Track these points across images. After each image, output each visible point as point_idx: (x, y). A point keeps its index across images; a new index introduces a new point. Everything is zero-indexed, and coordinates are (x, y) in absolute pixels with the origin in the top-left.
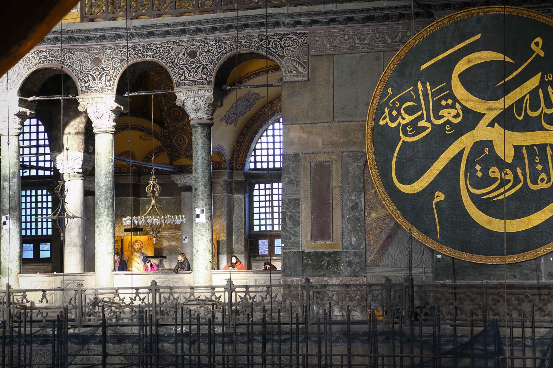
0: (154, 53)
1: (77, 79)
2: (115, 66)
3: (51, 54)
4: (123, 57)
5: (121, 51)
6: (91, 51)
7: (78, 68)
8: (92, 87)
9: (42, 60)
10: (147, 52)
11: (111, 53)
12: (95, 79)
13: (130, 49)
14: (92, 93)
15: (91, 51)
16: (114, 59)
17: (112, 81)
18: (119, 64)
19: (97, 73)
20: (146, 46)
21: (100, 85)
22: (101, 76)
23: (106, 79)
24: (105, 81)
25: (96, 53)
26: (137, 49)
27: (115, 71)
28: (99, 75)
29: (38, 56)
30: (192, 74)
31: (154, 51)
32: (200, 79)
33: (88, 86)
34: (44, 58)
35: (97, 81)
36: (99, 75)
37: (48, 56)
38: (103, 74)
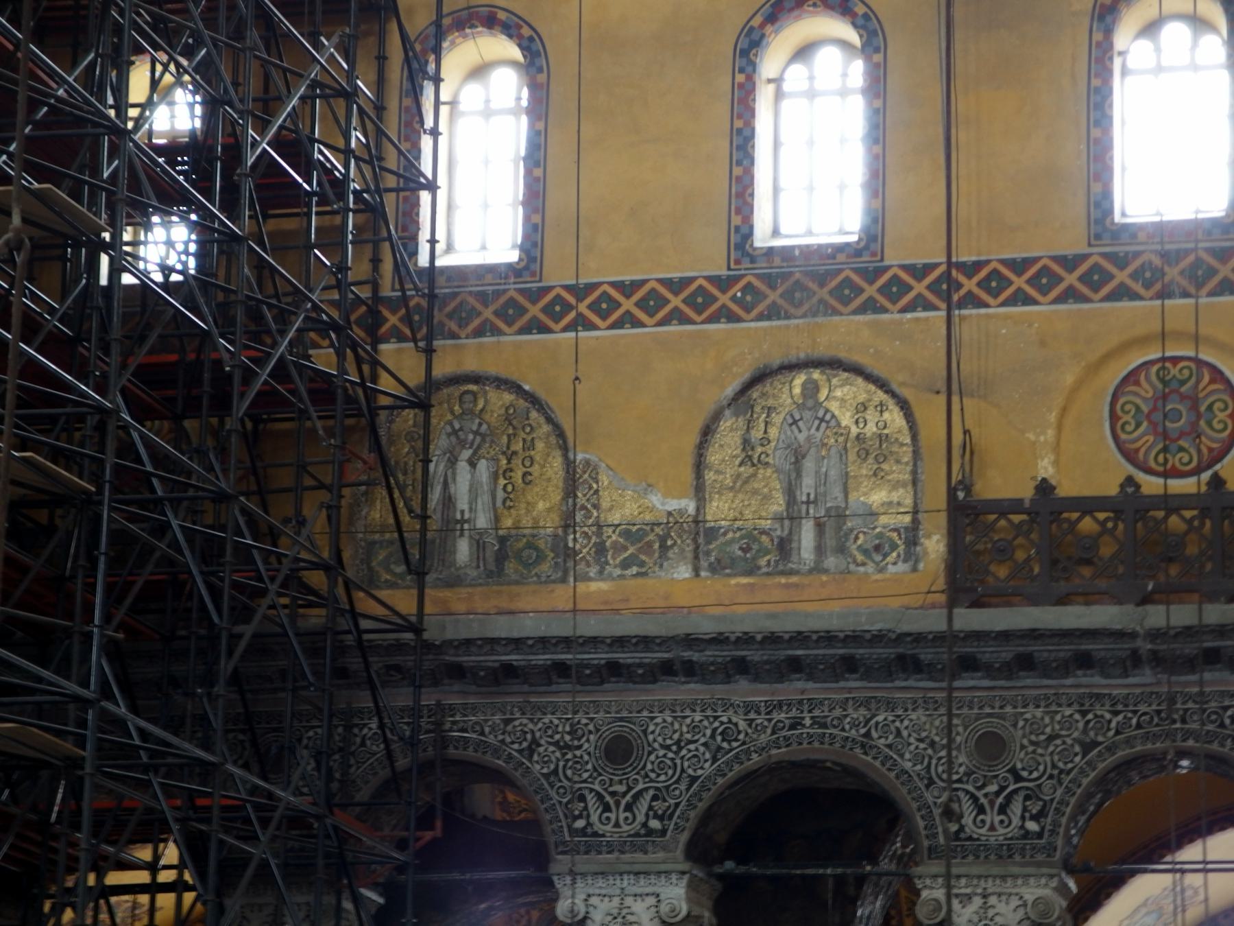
0: (1210, 727)
1: (915, 805)
2: (1061, 765)
3: (816, 713)
4: (1092, 734)
5: (1084, 713)
6: (971, 708)
7: (919, 767)
8: (970, 838)
9: (784, 733)
10: (1184, 721)
11: (1047, 720)
12: (981, 810)
13: (1120, 707)
14: (971, 858)
15: (971, 708)
16: (1058, 742)
17: (1049, 820)
18: (1077, 759)
19: (993, 788)
20: (1180, 700)
21: (1001, 831)
22: (1009, 799)
23: (1025, 809)
24: (1023, 818)
25: (989, 715)
26: (1147, 710)
27: (1060, 783)
28: (998, 794)
29: (770, 720)
30: (613, 816)
31: (1214, 717)
32: (637, 835)
33: (957, 832)
34: (793, 727)
35: (992, 817)
36: (998, 794)
37: (808, 722)
38: (1015, 791)
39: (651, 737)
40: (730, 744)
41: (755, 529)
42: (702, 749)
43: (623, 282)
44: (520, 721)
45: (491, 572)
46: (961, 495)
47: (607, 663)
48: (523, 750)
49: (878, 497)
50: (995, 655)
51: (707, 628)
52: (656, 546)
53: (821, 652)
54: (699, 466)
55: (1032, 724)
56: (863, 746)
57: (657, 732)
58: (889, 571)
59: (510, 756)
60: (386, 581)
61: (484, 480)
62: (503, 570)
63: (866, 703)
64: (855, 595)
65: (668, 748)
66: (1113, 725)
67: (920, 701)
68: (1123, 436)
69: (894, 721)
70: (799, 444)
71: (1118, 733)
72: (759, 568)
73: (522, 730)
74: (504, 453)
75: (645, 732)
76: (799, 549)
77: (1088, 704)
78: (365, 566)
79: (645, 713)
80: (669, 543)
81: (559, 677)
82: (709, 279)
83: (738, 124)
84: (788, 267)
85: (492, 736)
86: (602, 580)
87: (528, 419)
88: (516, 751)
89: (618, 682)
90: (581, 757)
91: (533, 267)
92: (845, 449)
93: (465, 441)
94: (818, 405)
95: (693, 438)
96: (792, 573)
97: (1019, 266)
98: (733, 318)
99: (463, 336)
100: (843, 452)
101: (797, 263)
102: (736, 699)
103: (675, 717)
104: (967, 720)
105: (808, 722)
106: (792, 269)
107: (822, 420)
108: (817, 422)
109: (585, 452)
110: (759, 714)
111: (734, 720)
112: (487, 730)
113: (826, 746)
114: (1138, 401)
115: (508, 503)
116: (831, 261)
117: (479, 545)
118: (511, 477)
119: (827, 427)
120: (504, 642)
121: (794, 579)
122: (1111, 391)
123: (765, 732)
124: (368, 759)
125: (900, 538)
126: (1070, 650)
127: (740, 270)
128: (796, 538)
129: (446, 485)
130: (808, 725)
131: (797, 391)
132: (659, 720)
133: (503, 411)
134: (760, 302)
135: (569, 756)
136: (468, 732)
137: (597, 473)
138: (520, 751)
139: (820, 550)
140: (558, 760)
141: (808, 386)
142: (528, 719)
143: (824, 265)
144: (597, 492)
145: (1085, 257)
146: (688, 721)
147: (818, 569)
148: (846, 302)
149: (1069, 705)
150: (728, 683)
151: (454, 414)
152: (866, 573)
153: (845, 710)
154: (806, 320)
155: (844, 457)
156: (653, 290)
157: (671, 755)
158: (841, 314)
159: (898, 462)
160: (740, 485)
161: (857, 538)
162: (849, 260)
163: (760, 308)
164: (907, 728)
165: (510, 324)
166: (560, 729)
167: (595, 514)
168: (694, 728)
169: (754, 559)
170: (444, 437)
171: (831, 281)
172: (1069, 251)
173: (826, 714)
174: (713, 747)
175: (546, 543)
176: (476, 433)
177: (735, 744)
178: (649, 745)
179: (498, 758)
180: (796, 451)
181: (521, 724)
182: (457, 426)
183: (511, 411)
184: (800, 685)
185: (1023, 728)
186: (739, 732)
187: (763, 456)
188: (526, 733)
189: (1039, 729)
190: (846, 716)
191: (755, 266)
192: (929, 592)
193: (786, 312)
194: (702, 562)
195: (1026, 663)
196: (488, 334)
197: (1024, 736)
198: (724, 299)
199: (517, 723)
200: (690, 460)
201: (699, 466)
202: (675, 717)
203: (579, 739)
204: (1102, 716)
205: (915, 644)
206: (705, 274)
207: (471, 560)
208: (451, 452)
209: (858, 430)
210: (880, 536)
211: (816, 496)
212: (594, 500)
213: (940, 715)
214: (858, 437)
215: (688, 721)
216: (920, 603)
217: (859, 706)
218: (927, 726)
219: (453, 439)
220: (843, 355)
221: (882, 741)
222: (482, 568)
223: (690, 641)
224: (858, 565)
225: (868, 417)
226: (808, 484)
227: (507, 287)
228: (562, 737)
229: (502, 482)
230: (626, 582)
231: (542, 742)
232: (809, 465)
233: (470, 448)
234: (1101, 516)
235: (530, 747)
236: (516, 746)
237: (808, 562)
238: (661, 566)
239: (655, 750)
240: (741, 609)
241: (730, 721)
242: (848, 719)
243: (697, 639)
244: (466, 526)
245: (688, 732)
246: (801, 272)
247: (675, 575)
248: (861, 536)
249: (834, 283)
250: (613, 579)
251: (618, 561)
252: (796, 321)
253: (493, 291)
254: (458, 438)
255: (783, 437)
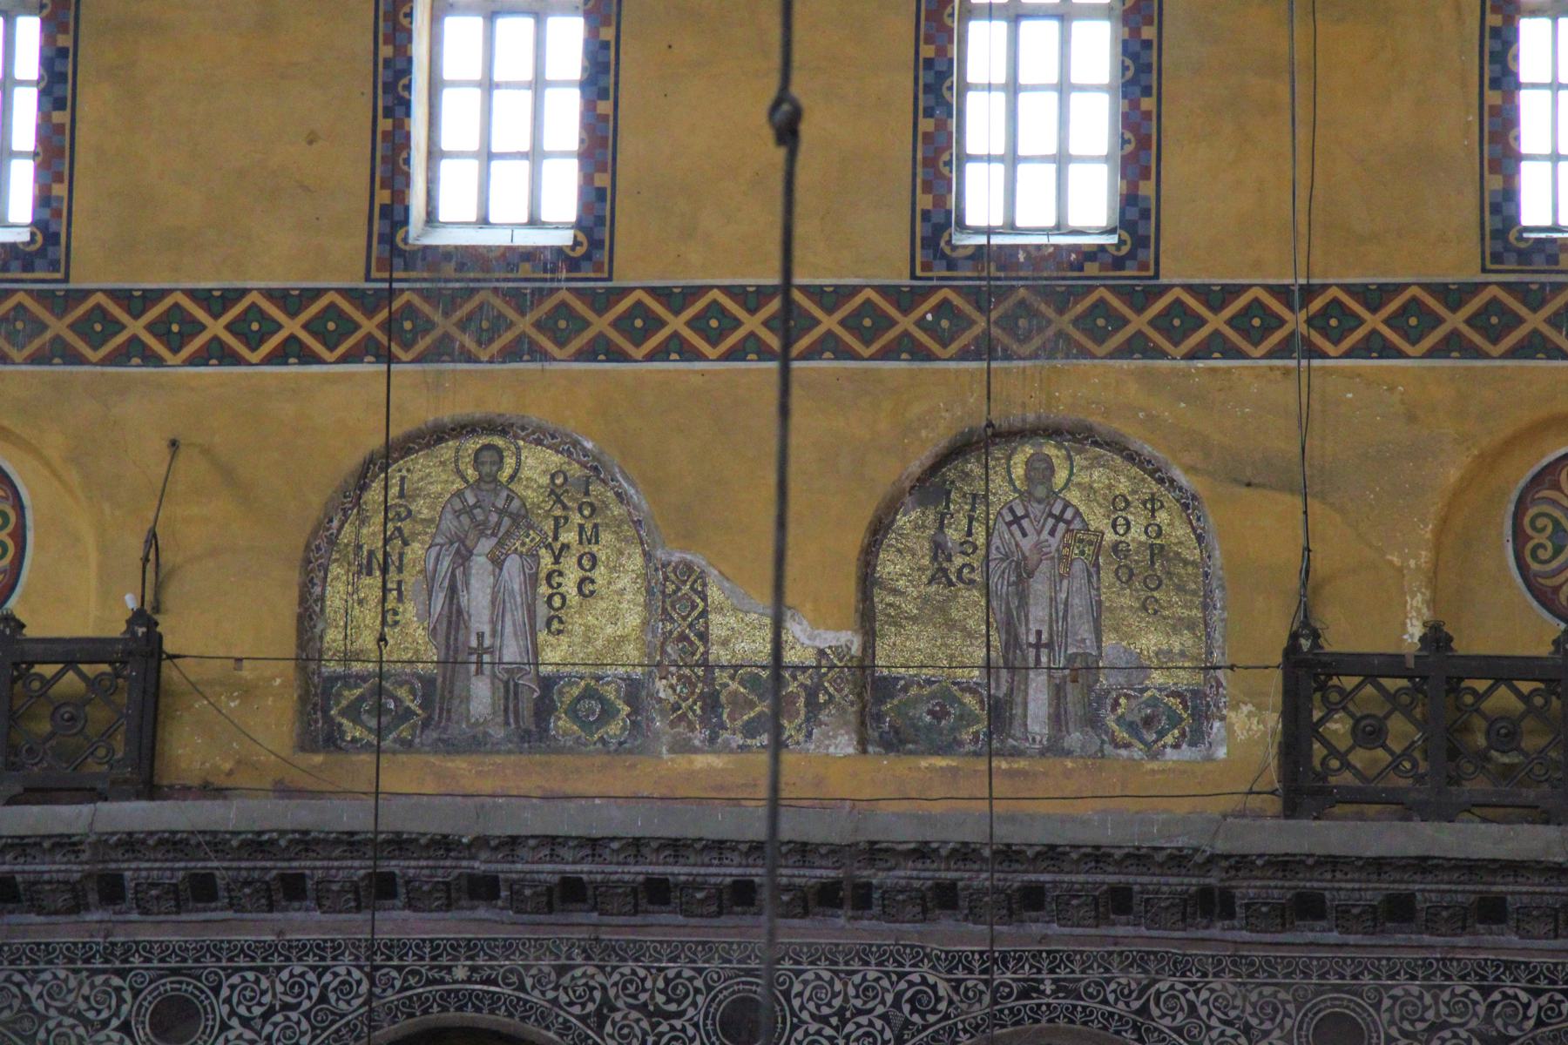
3: (1062, 973)
4: (1499, 1023)
5: (1485, 992)
6: (1307, 975)
9: (1010, 1003)
11: (1428, 999)
13: (1543, 984)
25: (1336, 988)
34: (1024, 994)
37: (1048, 987)
39: (796, 1003)
40: (924, 1018)
41: (954, 683)
42: (879, 1024)
43: (744, 287)
44: (583, 970)
45: (528, 732)
46: (1305, 644)
47: (735, 882)
48: (588, 1015)
49: (1150, 641)
50: (1357, 895)
51: (906, 834)
52: (801, 702)
53: (1081, 878)
54: (867, 581)
55: (1403, 1005)
56: (1136, 1028)
57: (807, 994)
58: (1167, 757)
59: (567, 1026)
60: (354, 740)
61: (516, 587)
62: (547, 730)
63: (1141, 961)
64: (1118, 792)
65: (825, 1020)
66: (1533, 1011)
67: (1226, 962)
68: (1535, 566)
69: (1184, 992)
70: (1023, 554)
71: (1540, 1023)
72: (961, 744)
73: (586, 984)
74: (549, 547)
75: (787, 994)
76: (1025, 716)
77: (1491, 977)
78: (319, 714)
79: (787, 964)
80: (822, 698)
81: (651, 902)
82: (882, 290)
83: (928, 51)
84: (1006, 279)
85: (536, 993)
86: (714, 752)
87: (587, 493)
88: (577, 1017)
89: (744, 913)
90: (684, 1030)
91: (1141, 254)
92: (1097, 565)
93: (485, 522)
94: (1053, 495)
95: (855, 539)
96: (1016, 753)
97: (1374, 296)
98: (920, 353)
99: (486, 359)
100: (1093, 570)
101: (1022, 274)
102: (933, 947)
103: (836, 973)
104: (1301, 993)
105: (1048, 987)
106: (1014, 283)
107: (1059, 519)
108: (1051, 521)
109: (684, 550)
110: (971, 972)
111: (931, 979)
112: (529, 982)
113: (1078, 1026)
114: (1558, 514)
115: (555, 625)
116: (1076, 274)
117: (509, 691)
118: (560, 585)
119: (1068, 531)
120: (532, 842)
121: (1021, 764)
122: (1514, 495)
123: (980, 1001)
124: (333, 1022)
125: (1185, 708)
126: (1474, 892)
127: (930, 279)
128: (1019, 699)
129: (453, 590)
130: (1048, 992)
131: (1019, 471)
132: (810, 976)
133: (545, 480)
134: (964, 330)
135: (664, 1027)
136: (498, 985)
137: (704, 585)
138: (583, 1019)
139: (1057, 719)
140: (645, 1033)
141: (1037, 465)
142: (597, 966)
143: (1064, 278)
144: (704, 614)
145: (1478, 287)
146: (857, 979)
147: (1054, 749)
148: (1100, 337)
149: (1463, 978)
150: (924, 920)
151: (467, 481)
152: (1131, 759)
153: (1107, 970)
154: (1038, 362)
155: (1094, 579)
156: (1414, 299)
157: (828, 1031)
158: (1094, 357)
159: (1180, 589)
160: (938, 613)
161: (1116, 704)
162: (1103, 274)
163: (965, 339)
164: (1205, 1002)
165: (561, 344)
166: (648, 984)
167: (702, 649)
168: (865, 990)
169: (953, 729)
170: (449, 516)
171: (1076, 303)
172: (1453, 278)
173: (1078, 976)
174: (898, 1022)
175: (618, 691)
176: (502, 512)
177: (931, 1018)
178: (793, 1014)
179: (547, 1028)
180: (1018, 564)
181: (584, 974)
182: (471, 500)
183: (559, 481)
184: (1036, 929)
185: (1390, 1009)
186: (939, 999)
187: (965, 571)
188: (592, 989)
189: (1415, 1012)
190: (1108, 981)
191: (954, 274)
192: (1251, 792)
193: (1005, 350)
194: (870, 731)
195: (1400, 910)
196: (674, 356)
197: (1392, 1022)
198: (906, 323)
199: (578, 973)
200: (852, 569)
201: (867, 581)
202: (836, 973)
203: (679, 1003)
204: (1516, 997)
205: (1233, 873)
206: (876, 282)
207: (494, 713)
208: (463, 542)
209: (1117, 537)
210: (1154, 702)
211: (1051, 635)
212: (700, 626)
213: (1259, 985)
214: (1115, 547)
215: (857, 979)
216: (1240, 806)
217: (1131, 965)
218: (1238, 1002)
219: (465, 519)
220: (1095, 420)
221: (1167, 1021)
222: (513, 726)
223: (874, 853)
224: (1117, 746)
225: (1130, 517)
226: (1038, 617)
227: (555, 285)
228: (652, 997)
229: (544, 589)
230: (751, 757)
231: (620, 1004)
232: (1039, 586)
233: (494, 535)
234: (1525, 687)
235: (599, 1010)
236: (577, 1010)
237: (1038, 738)
238: (809, 735)
239: (802, 1022)
240: (938, 808)
241: (924, 981)
242: (1113, 986)
243: (886, 850)
244: (486, 658)
245: (857, 996)
246: (1026, 287)
247: (832, 750)
248: (1122, 701)
249: (1080, 308)
250: (731, 751)
251: (739, 723)
252: (1021, 364)
253: (533, 291)
254: (473, 518)
255: (996, 541)
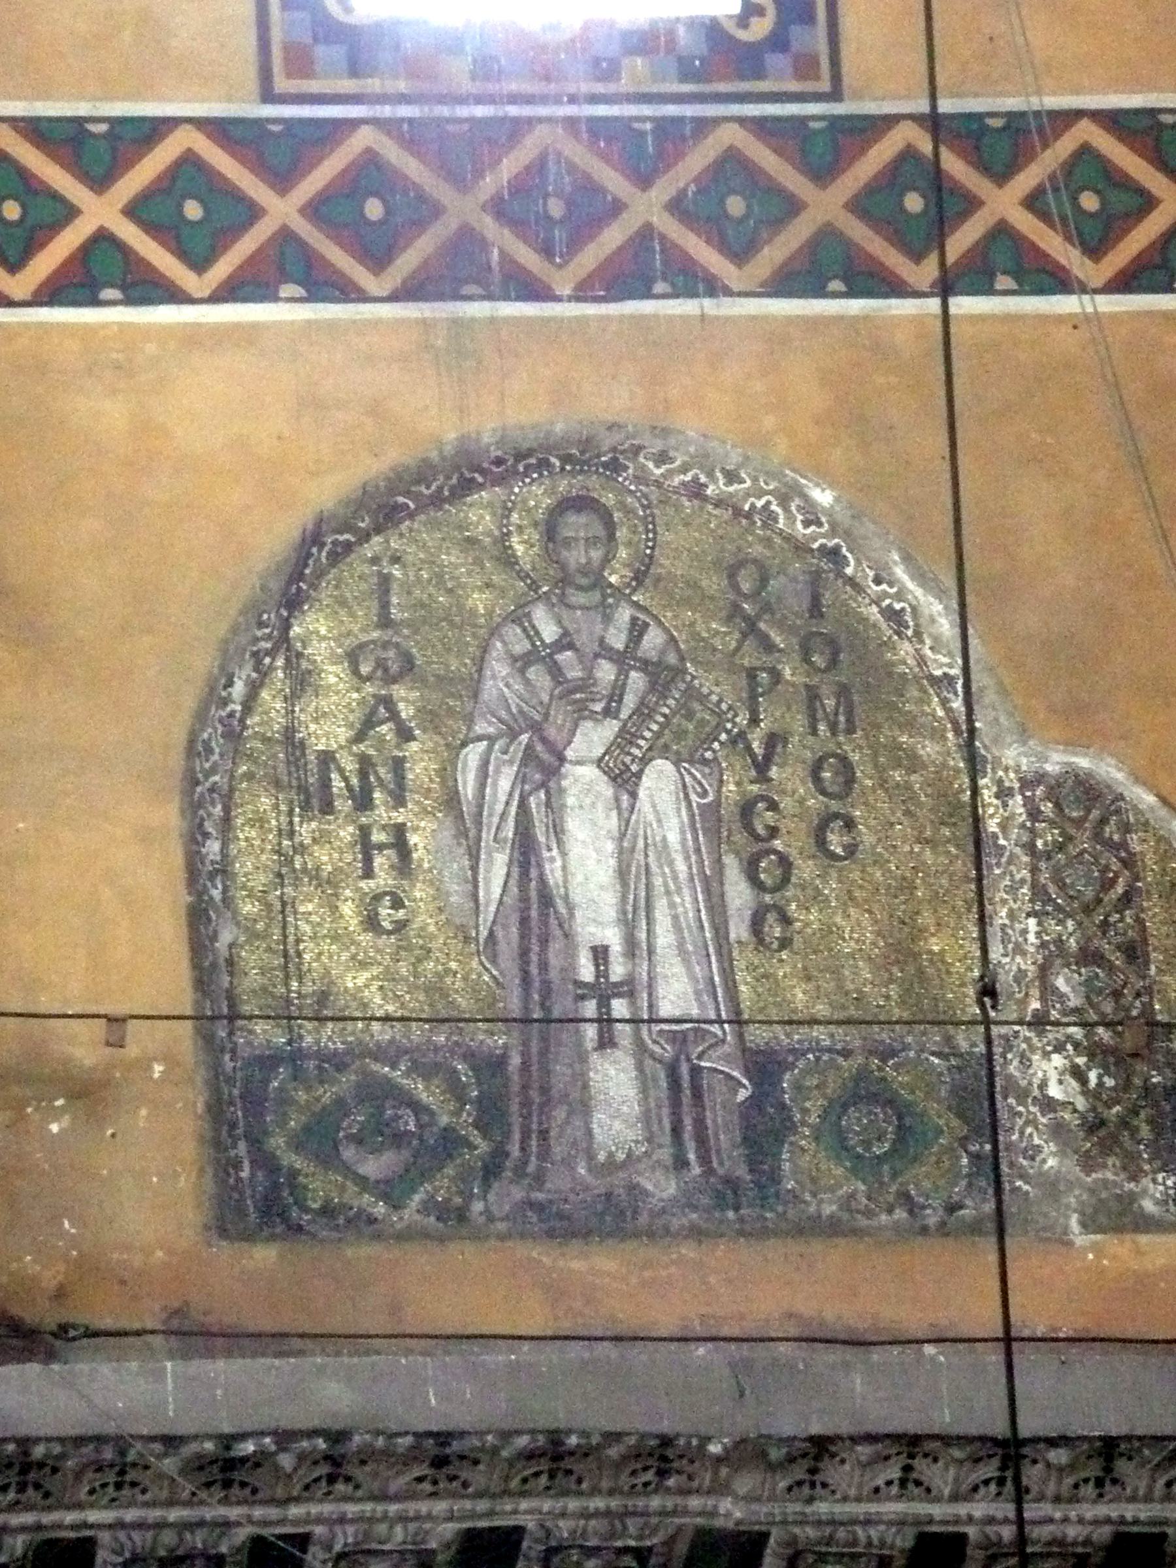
45: (731, 1182)
60: (328, 1211)
61: (673, 838)
62: (775, 1177)
78: (242, 1147)
93: (586, 684)
109: (1070, 744)
165: (740, 255)
208: (536, 728)
222: (697, 1170)
233: (607, 712)
244: (619, 1008)
254: (556, 672)
